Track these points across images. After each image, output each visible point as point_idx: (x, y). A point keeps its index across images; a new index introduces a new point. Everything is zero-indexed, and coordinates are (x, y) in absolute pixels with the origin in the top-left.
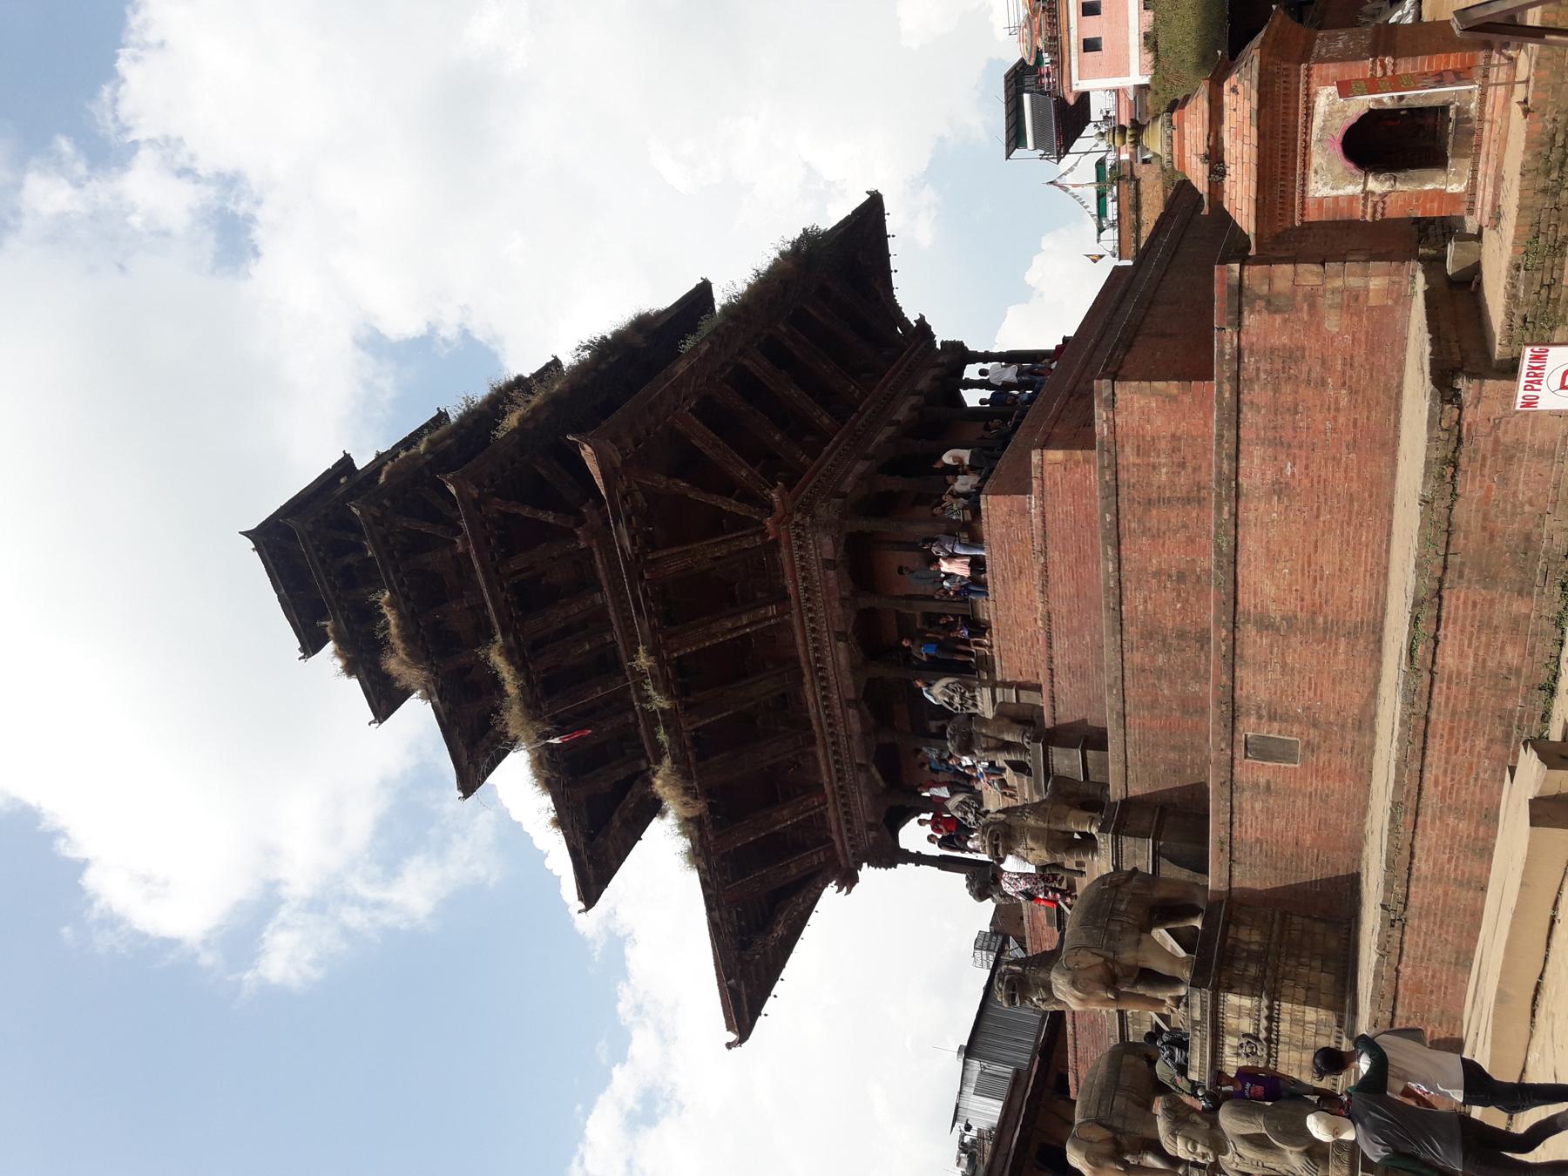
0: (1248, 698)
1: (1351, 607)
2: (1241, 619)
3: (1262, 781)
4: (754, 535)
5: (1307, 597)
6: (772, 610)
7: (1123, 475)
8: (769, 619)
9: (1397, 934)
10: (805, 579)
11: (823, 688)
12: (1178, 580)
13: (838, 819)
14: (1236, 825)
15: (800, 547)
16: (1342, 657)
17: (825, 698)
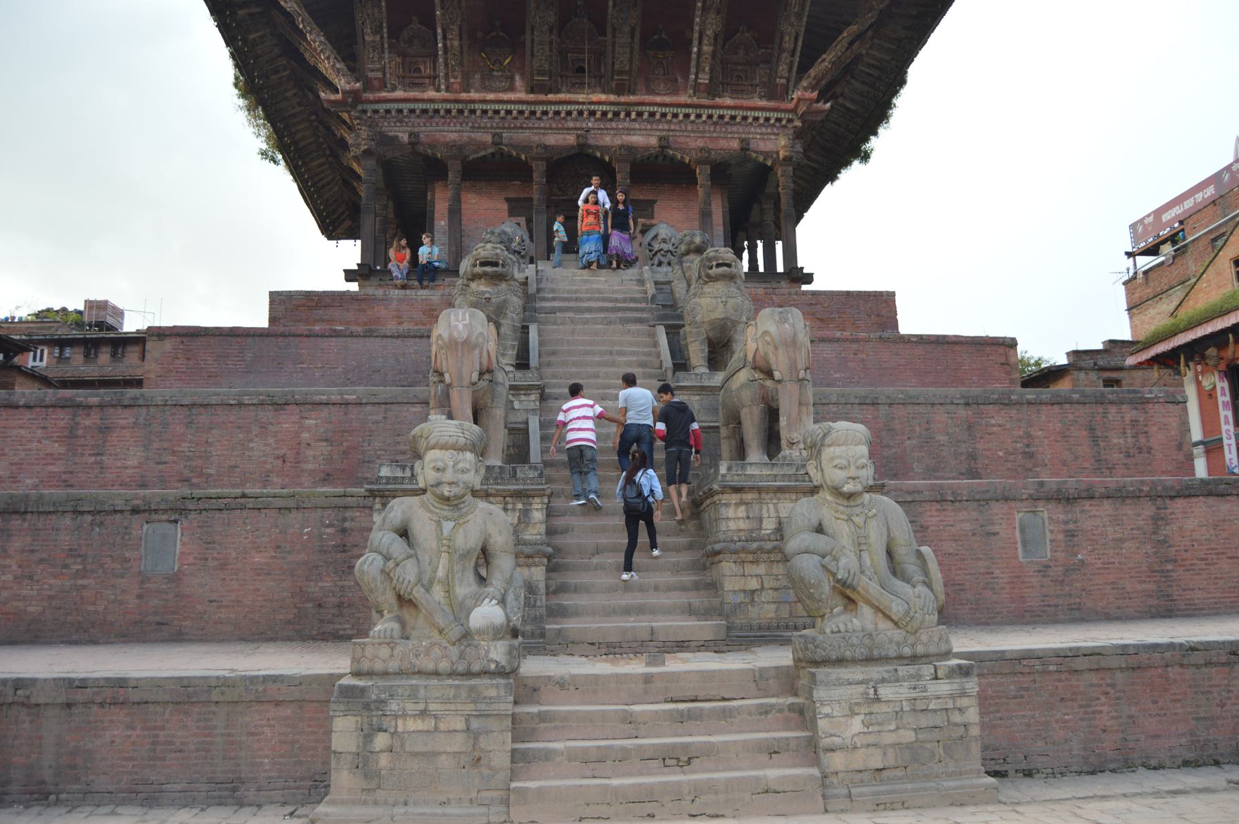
0: (1083, 511)
1: (1184, 590)
2: (1159, 502)
3: (996, 528)
4: (788, 81)
5: (1189, 554)
6: (704, 79)
7: (1113, 410)
8: (697, 75)
9: (1223, 659)
10: (733, 118)
11: (604, 114)
12: (1024, 453)
13: (431, 101)
14: (938, 506)
15: (767, 119)
16: (1139, 587)
17: (593, 113)
